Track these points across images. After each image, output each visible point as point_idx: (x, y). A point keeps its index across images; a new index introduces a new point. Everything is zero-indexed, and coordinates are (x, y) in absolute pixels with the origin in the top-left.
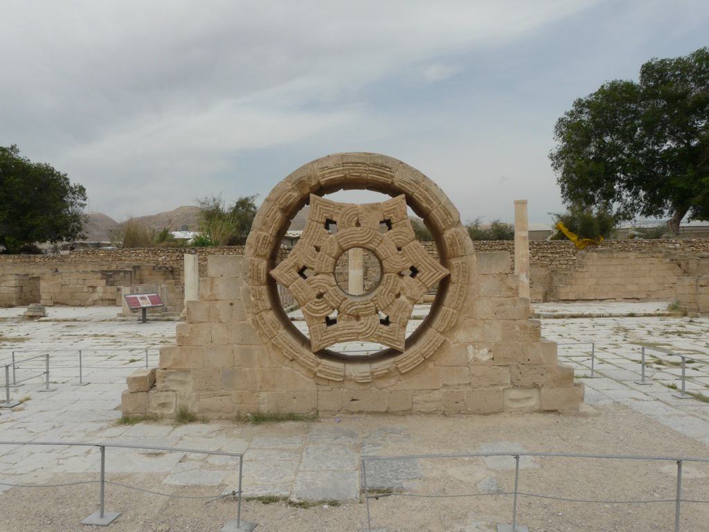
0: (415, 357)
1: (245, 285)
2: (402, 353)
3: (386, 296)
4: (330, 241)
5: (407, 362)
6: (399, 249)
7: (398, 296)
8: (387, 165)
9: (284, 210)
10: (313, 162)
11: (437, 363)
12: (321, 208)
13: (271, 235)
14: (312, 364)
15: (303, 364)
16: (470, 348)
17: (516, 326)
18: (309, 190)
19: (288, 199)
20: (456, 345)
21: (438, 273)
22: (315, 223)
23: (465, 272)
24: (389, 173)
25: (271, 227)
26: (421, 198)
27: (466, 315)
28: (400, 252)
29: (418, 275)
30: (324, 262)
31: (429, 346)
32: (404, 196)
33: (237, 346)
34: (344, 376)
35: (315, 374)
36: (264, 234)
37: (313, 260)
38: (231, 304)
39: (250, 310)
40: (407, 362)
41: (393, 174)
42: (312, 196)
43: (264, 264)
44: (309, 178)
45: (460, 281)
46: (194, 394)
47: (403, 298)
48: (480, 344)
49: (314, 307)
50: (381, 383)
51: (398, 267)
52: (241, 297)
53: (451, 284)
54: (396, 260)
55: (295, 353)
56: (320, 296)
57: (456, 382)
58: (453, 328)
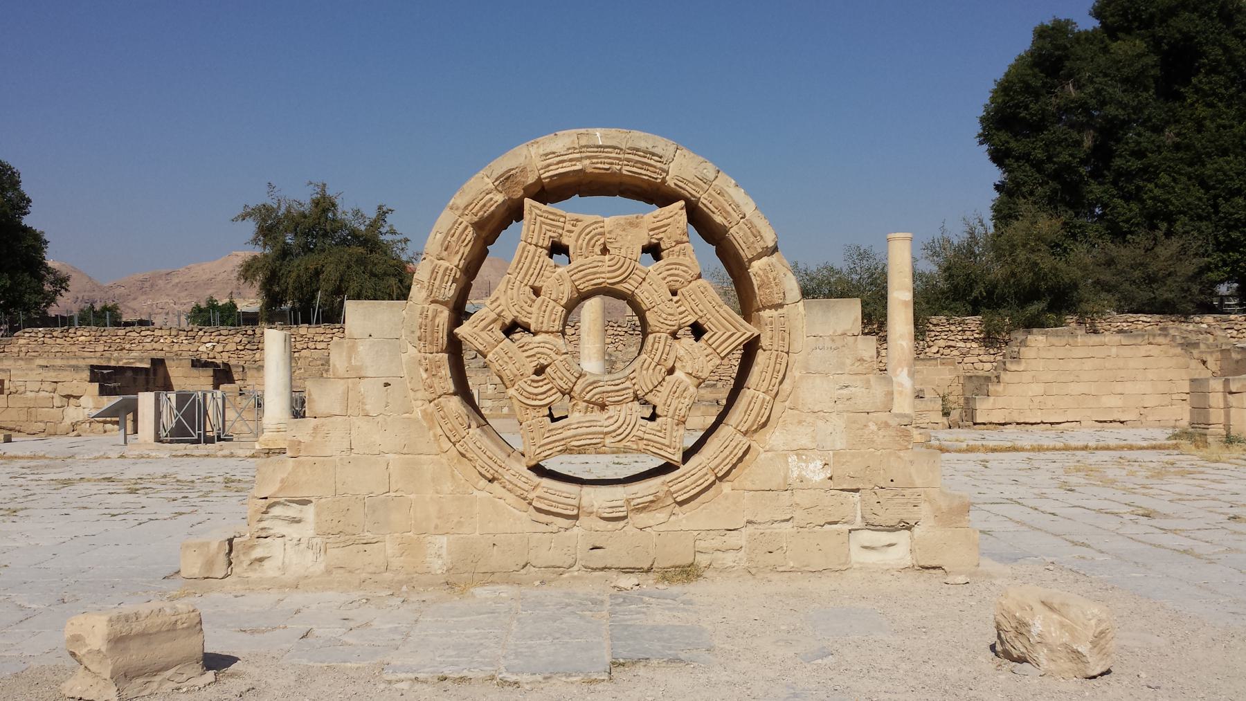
0: (700, 473)
1: (412, 351)
2: (678, 468)
3: (650, 371)
4: (559, 279)
5: (687, 482)
6: (674, 293)
7: (671, 371)
8: (655, 150)
9: (478, 226)
11: (736, 483)
12: (543, 223)
13: (457, 266)
14: (526, 487)
15: (510, 486)
17: (870, 424)
18: (522, 193)
20: (770, 454)
21: (739, 334)
22: (532, 248)
23: (785, 332)
24: (659, 165)
25: (457, 252)
26: (710, 206)
27: (787, 404)
28: (675, 299)
29: (706, 336)
30: (547, 313)
31: (723, 456)
32: (682, 203)
33: (397, 456)
35: (530, 504)
36: (445, 264)
37: (529, 310)
38: (387, 385)
39: (420, 395)
40: (687, 482)
41: (665, 167)
42: (528, 202)
43: (444, 315)
44: (523, 170)
45: (775, 347)
46: (318, 540)
47: (679, 374)
48: (809, 453)
49: (530, 389)
51: (674, 322)
52: (404, 373)
53: (760, 351)
54: (670, 311)
55: (496, 467)
56: (540, 371)
57: (767, 518)
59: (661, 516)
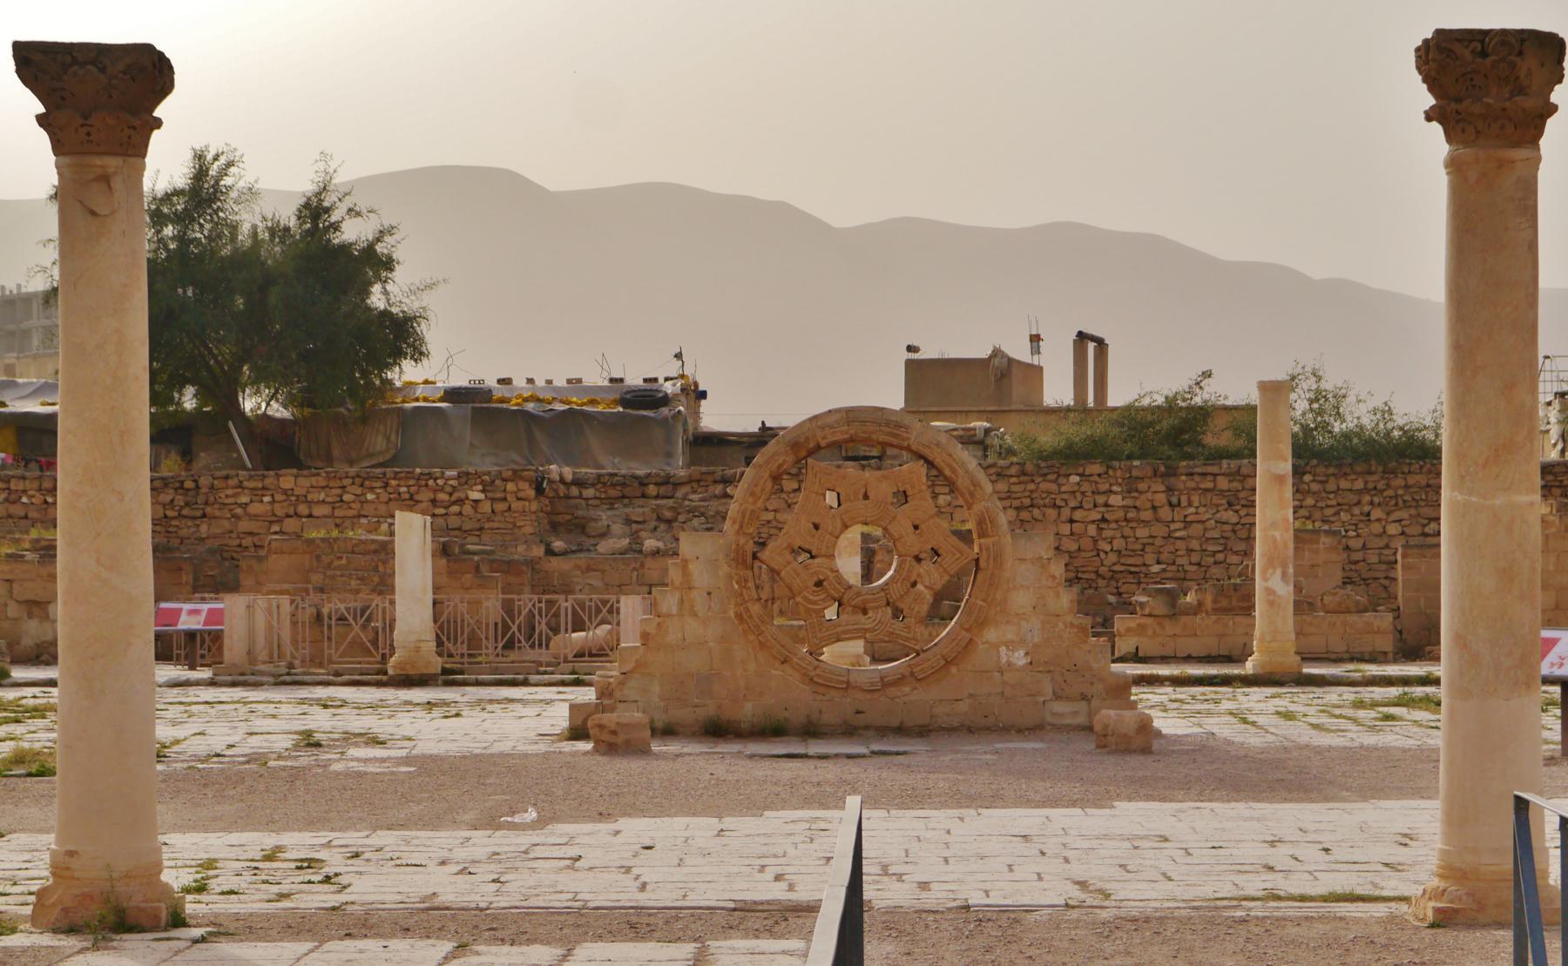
1: (726, 568)
6: (916, 527)
7: (914, 584)
10: (811, 420)
16: (1003, 650)
19: (780, 466)
23: (998, 557)
34: (848, 682)
44: (807, 439)
47: (920, 587)
50: (892, 691)
56: (819, 584)
58: (982, 624)
59: (907, 689)
